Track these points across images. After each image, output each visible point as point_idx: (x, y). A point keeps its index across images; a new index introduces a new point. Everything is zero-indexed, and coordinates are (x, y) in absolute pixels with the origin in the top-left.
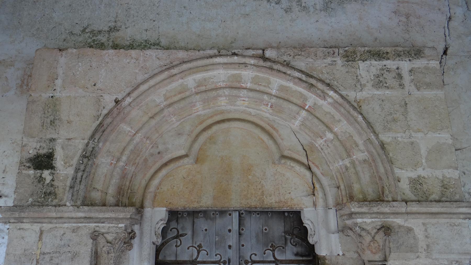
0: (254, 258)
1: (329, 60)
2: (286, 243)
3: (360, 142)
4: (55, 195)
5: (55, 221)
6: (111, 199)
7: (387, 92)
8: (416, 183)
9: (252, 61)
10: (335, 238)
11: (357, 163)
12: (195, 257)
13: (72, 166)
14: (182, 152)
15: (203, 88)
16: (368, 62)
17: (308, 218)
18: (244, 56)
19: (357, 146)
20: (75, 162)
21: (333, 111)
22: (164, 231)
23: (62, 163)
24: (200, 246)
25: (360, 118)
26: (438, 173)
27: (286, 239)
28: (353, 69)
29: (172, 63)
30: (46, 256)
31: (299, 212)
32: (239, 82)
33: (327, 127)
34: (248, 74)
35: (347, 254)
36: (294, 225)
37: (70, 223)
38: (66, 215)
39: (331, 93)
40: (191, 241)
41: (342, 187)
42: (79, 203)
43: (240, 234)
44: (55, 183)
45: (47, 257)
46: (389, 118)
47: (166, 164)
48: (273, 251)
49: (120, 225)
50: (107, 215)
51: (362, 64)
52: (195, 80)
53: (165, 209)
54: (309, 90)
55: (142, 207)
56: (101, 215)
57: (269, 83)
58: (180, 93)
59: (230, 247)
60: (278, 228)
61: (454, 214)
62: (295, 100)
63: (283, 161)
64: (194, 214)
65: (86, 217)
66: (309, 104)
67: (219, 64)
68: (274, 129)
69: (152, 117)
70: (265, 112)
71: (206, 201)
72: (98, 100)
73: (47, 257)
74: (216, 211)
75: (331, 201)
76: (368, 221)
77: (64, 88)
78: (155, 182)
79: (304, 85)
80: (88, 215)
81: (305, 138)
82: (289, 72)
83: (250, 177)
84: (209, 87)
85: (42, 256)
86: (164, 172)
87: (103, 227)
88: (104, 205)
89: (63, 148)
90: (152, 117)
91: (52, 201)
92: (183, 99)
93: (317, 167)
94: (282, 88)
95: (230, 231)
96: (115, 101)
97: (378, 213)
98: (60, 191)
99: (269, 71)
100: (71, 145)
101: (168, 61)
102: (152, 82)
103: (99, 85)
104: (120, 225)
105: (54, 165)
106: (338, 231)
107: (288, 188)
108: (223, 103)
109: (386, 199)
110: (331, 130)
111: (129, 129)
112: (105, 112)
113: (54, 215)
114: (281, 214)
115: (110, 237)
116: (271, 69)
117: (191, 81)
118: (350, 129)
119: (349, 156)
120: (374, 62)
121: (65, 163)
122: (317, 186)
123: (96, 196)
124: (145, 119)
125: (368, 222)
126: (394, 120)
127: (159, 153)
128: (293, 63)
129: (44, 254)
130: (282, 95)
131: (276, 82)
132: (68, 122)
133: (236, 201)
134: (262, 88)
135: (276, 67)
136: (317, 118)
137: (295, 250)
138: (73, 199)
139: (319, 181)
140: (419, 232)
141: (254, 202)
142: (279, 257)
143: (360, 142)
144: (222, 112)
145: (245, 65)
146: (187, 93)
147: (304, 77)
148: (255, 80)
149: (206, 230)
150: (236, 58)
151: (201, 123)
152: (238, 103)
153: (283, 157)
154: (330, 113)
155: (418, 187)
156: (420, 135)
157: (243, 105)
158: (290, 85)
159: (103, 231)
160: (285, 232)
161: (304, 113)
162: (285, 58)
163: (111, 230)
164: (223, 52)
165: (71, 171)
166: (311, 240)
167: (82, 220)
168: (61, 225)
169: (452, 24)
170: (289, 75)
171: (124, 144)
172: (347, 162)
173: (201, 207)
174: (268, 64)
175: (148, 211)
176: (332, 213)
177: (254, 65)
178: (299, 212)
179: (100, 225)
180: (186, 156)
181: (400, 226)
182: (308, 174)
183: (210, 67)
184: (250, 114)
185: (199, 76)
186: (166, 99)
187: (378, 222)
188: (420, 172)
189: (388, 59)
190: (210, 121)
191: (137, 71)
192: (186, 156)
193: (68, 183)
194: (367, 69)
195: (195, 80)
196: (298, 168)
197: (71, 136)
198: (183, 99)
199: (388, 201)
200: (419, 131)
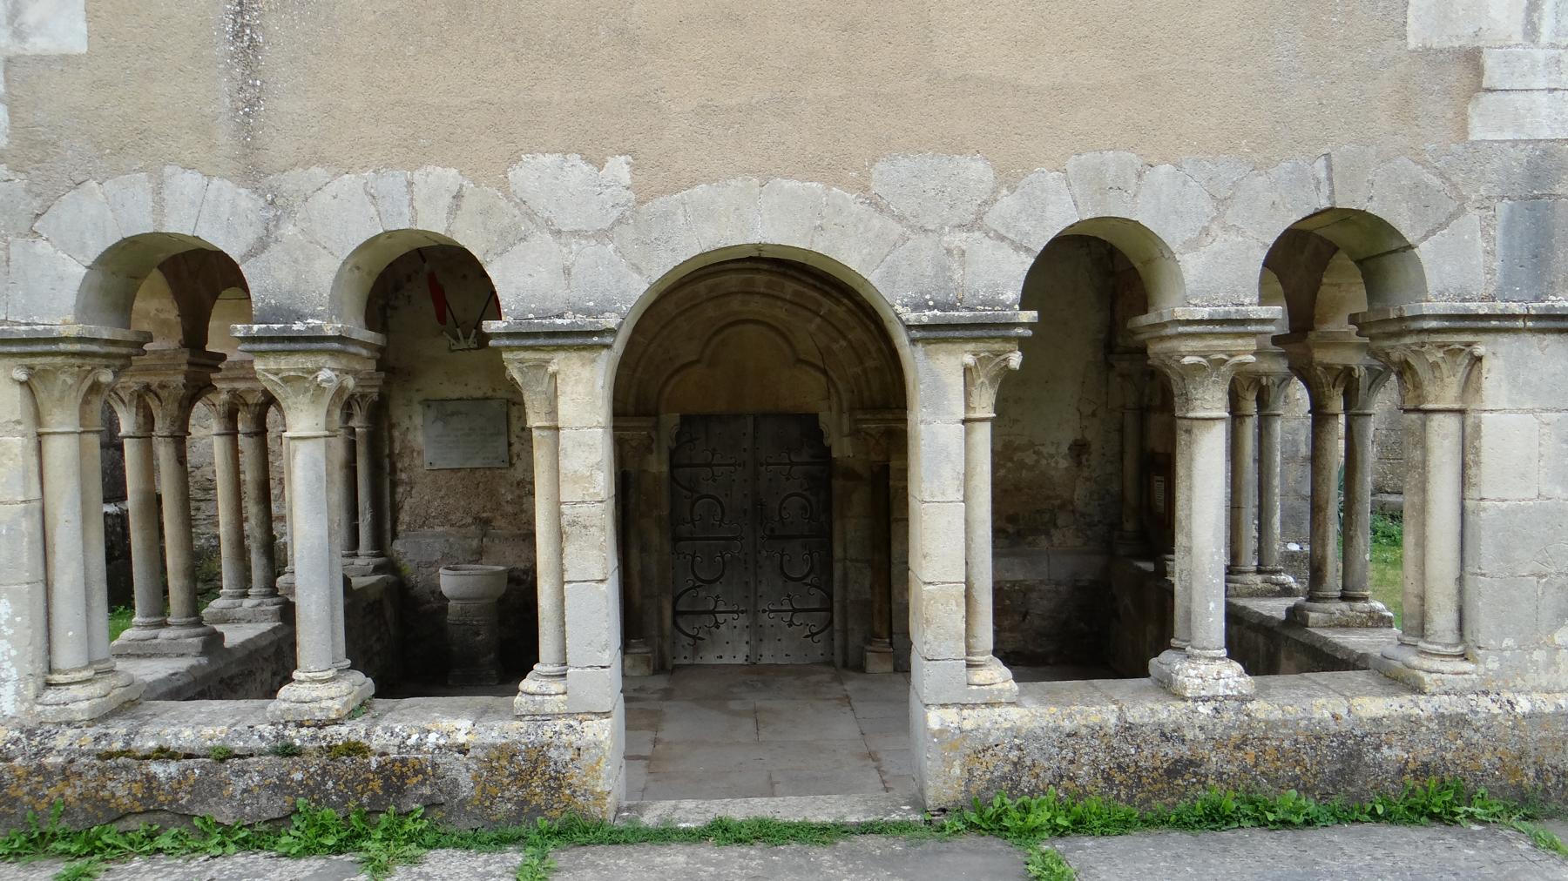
3: (873, 349)
9: (766, 267)
10: (846, 441)
17: (827, 419)
22: (678, 435)
25: (872, 327)
33: (841, 333)
36: (809, 426)
47: (677, 371)
55: (656, 414)
69: (663, 327)
75: (845, 405)
78: (668, 389)
86: (676, 378)
90: (663, 327)
92: (694, 306)
94: (796, 293)
106: (850, 435)
108: (735, 304)
110: (845, 337)
115: (634, 444)
116: (785, 275)
119: (861, 363)
135: (790, 272)
136: (834, 326)
139: (835, 385)
142: (794, 459)
143: (873, 349)
145: (758, 270)
153: (799, 361)
157: (756, 306)
161: (818, 320)
166: (827, 443)
172: (858, 370)
175: (663, 417)
176: (845, 417)
180: (698, 361)
182: (823, 379)
185: (710, 282)
187: (882, 426)
192: (698, 361)
196: (812, 371)
198: (694, 306)
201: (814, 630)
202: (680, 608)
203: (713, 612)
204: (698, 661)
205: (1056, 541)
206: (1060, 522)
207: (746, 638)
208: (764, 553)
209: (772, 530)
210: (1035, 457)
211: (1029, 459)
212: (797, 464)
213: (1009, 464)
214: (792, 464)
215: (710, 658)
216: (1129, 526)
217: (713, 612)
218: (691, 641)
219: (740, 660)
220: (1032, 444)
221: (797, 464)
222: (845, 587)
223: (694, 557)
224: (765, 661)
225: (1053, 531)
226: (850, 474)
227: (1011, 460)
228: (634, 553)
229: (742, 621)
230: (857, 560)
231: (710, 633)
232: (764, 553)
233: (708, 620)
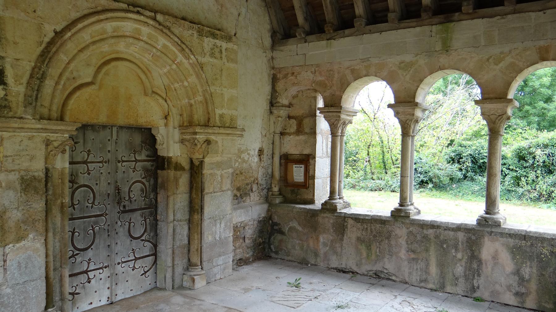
0: (124, 159)
1: (190, 32)
2: (142, 149)
4: (10, 108)
5: (19, 131)
6: (54, 115)
7: (215, 60)
8: (221, 116)
11: (197, 102)
12: (85, 159)
13: (22, 84)
14: (89, 80)
15: (115, 34)
16: (208, 39)
17: (161, 134)
18: (147, 17)
19: (198, 92)
20: (25, 80)
21: (190, 68)
23: (13, 80)
24: (89, 151)
26: (230, 112)
27: (142, 147)
28: (201, 42)
29: (96, 8)
30: (9, 158)
31: (150, 129)
32: (140, 35)
34: (145, 30)
35: (183, 156)
36: (148, 137)
37: (31, 132)
38: (27, 126)
39: (192, 57)
40: (83, 147)
41: (185, 115)
42: (38, 117)
44: (9, 98)
45: (10, 160)
46: (214, 77)
49: (65, 135)
50: (59, 128)
51: (206, 40)
52: (111, 26)
56: (54, 128)
57: (157, 40)
58: (101, 35)
59: (109, 151)
60: (137, 139)
61: (235, 134)
62: (170, 56)
63: (153, 95)
65: (42, 129)
66: (178, 60)
67: (131, 19)
68: (149, 71)
70: (147, 59)
71: (102, 119)
72: (40, 27)
73: (10, 160)
74: (100, 125)
75: (176, 124)
77: (7, 7)
79: (179, 48)
80: (44, 127)
81: (166, 81)
82: (172, 37)
83: (130, 103)
84: (120, 34)
85: (5, 159)
87: (53, 136)
88: (49, 119)
89: (12, 66)
90: (81, 51)
91: (7, 113)
93: (171, 101)
94: (165, 46)
95: (109, 140)
96: (54, 31)
98: (13, 105)
99: (161, 33)
100: (19, 65)
101: (93, 5)
102: (86, 22)
103: (39, 13)
104: (65, 135)
105: (6, 81)
107: (150, 113)
109: (210, 125)
111: (65, 58)
112: (47, 40)
113: (16, 125)
114: (130, 128)
116: (162, 31)
117: (109, 26)
118: (196, 81)
120: (212, 40)
121: (16, 81)
122: (170, 113)
123: (45, 111)
124: (76, 51)
125: (201, 137)
126: (216, 79)
127: (74, 78)
128: (172, 29)
129: (6, 157)
130: (164, 50)
131: (162, 41)
132: (14, 43)
133: (121, 121)
134: (152, 43)
135: (165, 30)
137: (147, 153)
138: (33, 115)
140: (220, 143)
141: (132, 122)
142: (138, 158)
144: (117, 52)
146: (105, 36)
147: (179, 43)
148: (150, 36)
149: (93, 139)
150: (142, 17)
151: (103, 58)
152: (132, 48)
153: (153, 92)
154: (187, 69)
155: (222, 119)
156: (225, 90)
158: (169, 45)
159: (52, 139)
160: (142, 142)
161: (174, 66)
162: (168, 24)
163: (59, 139)
164: (131, 8)
165: (22, 89)
166: (157, 147)
167: (41, 131)
168: (18, 134)
169: (241, 18)
170: (172, 38)
171: (59, 71)
173: (99, 123)
174: (161, 27)
176: (177, 131)
177: (152, 25)
178: (150, 129)
179: (50, 134)
181: (213, 140)
183: (126, 20)
184: (135, 57)
186: (92, 37)
188: (224, 111)
189: (217, 39)
190: (108, 58)
191: (70, 7)
193: (21, 98)
194: (208, 42)
195: (111, 26)
197: (18, 57)
199: (211, 126)
200: (225, 87)
201: (146, 269)
205: (252, 199)
206: (254, 189)
207: (108, 285)
209: (124, 207)
210: (248, 156)
212: (140, 161)
213: (240, 160)
214: (136, 161)
216: (276, 189)
217: (86, 272)
221: (140, 161)
222: (174, 239)
224: (119, 298)
225: (251, 194)
226: (178, 167)
228: (50, 234)
229: (106, 273)
230: (181, 221)
231: (84, 287)
232: (119, 223)
233: (83, 278)
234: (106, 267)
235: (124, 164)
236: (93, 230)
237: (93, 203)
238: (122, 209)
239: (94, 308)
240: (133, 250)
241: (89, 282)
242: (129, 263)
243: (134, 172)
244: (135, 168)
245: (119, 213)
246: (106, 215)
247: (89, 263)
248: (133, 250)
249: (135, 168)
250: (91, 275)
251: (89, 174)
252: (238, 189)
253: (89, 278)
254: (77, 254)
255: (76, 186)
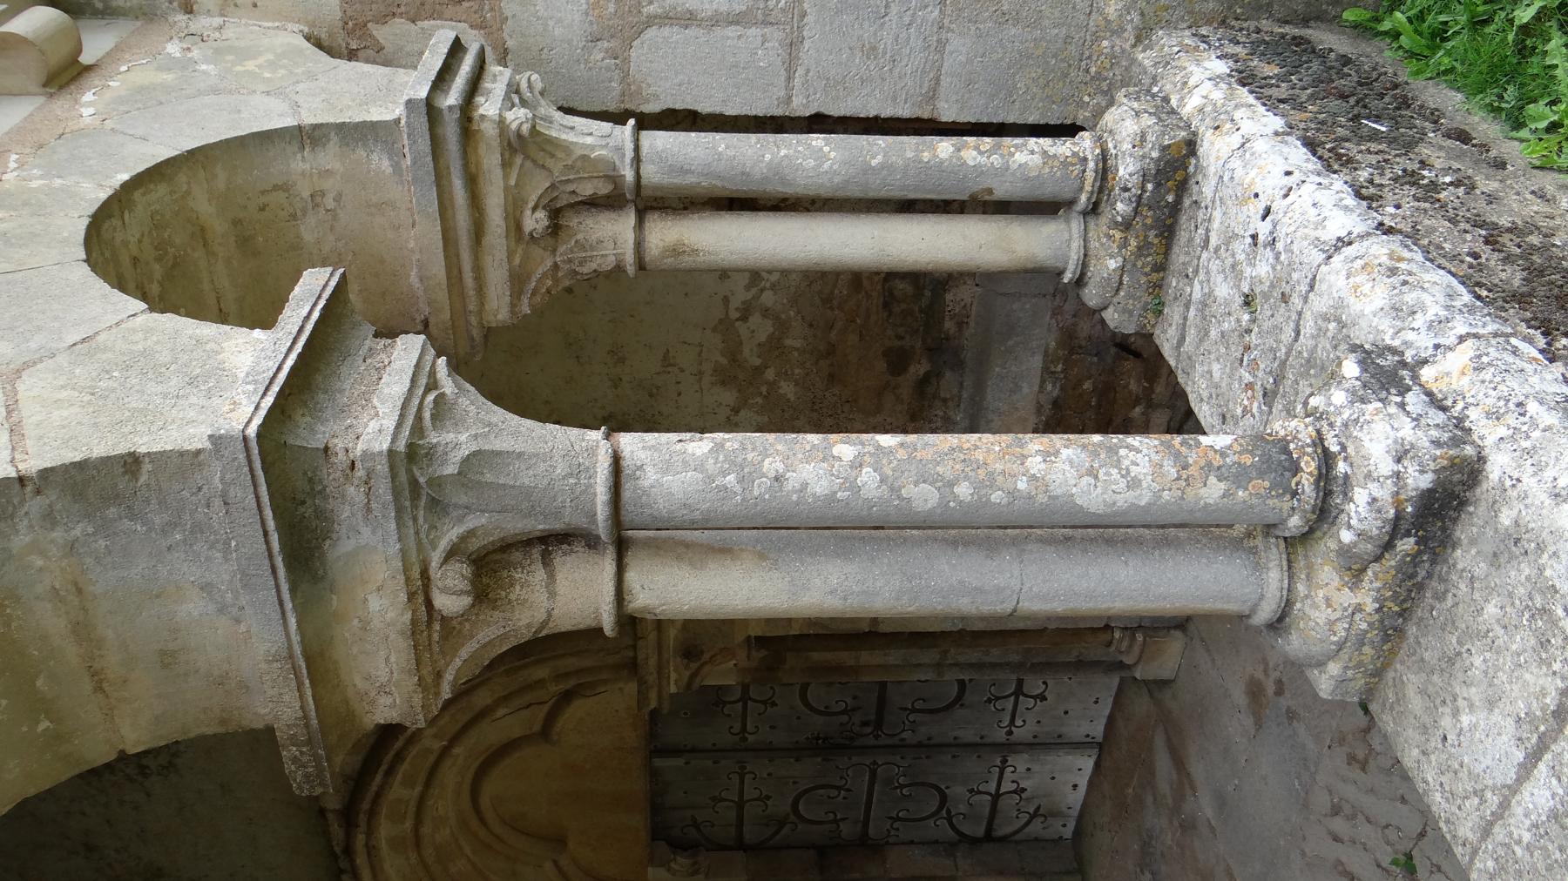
0: (737, 727)
9: (360, 839)
14: (548, 865)
24: (714, 799)
43: (693, 750)
48: (725, 703)
53: (650, 869)
54: (403, 760)
64: (656, 807)
76: (673, 676)
82: (374, 788)
97: (659, 673)
134: (412, 809)
145: (371, 850)
150: (358, 861)
153: (545, 733)
174: (362, 819)
192: (555, 863)
202: (980, 831)
203: (997, 796)
204: (1075, 813)
208: (904, 735)
209: (865, 724)
210: (756, 319)
211: (761, 329)
213: (770, 374)
215: (1076, 799)
218: (1037, 822)
219: (1087, 763)
220: (725, 326)
223: (898, 819)
227: (758, 371)
231: (1028, 800)
232: (904, 735)
234: (1004, 761)
235: (750, 728)
236: (902, 787)
237: (839, 788)
238: (869, 730)
239: (1091, 783)
240: (989, 701)
241: (1024, 790)
242: (1021, 708)
243: (774, 704)
244: (764, 703)
245: (877, 737)
246: (875, 763)
247: (979, 792)
248: (989, 701)
249: (764, 703)
250: (1007, 786)
251: (768, 798)
252: (898, 361)
253: (1015, 792)
254: (949, 812)
255: (792, 818)
